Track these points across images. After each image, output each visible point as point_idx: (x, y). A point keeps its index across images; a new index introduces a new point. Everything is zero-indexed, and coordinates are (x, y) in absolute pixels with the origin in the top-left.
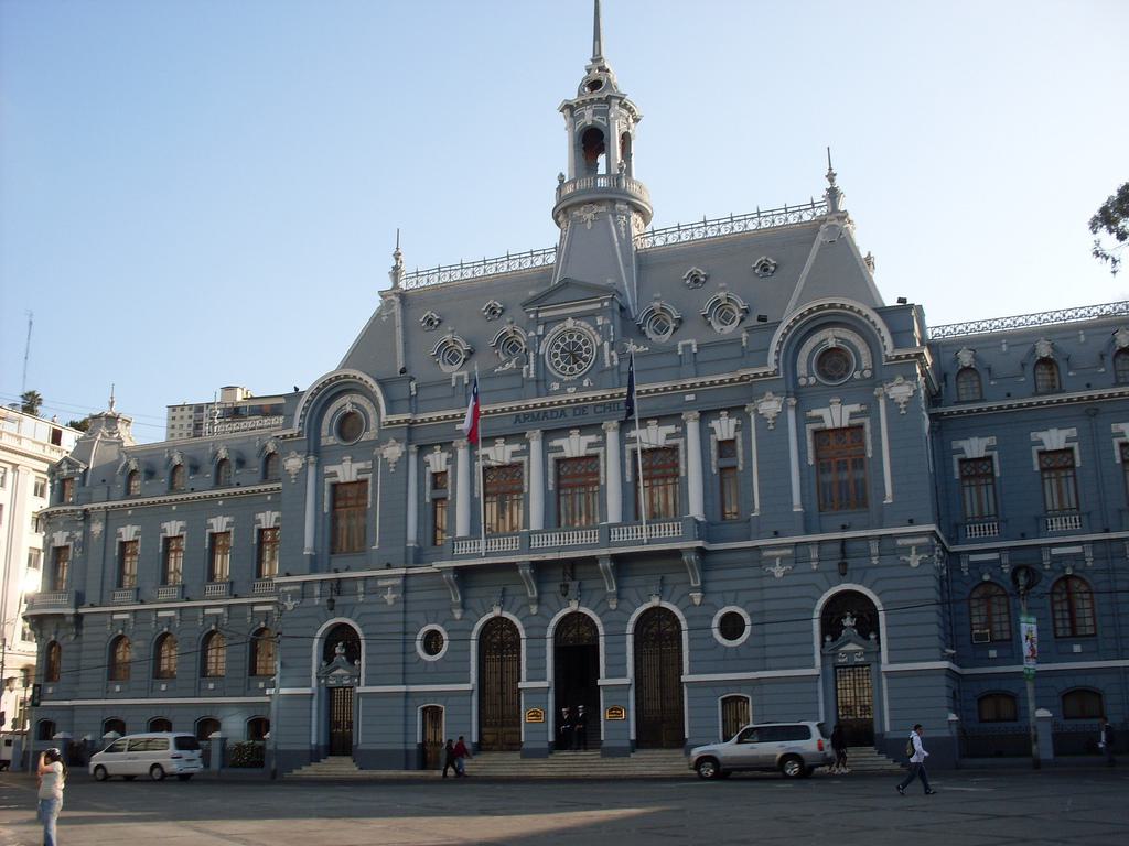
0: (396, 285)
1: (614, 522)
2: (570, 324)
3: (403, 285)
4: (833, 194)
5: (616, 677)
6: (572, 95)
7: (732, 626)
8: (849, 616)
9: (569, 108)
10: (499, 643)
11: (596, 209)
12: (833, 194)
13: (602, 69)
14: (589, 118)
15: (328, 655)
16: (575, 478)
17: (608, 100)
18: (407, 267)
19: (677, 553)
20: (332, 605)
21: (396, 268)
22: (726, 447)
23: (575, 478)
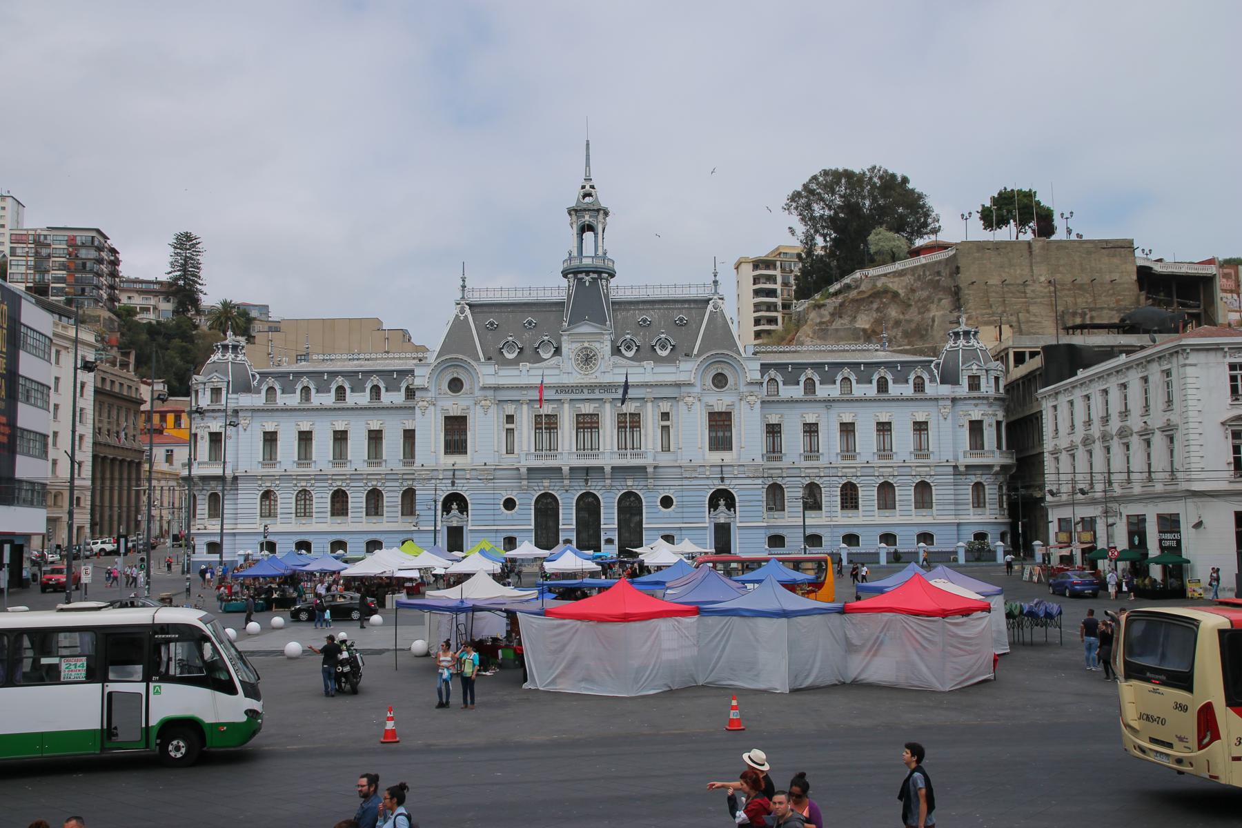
0: (463, 298)
1: (608, 451)
2: (586, 345)
3: (468, 294)
4: (715, 282)
5: (609, 521)
6: (573, 204)
7: (667, 502)
8: (721, 498)
9: (575, 211)
10: (546, 509)
11: (592, 275)
12: (715, 282)
13: (592, 187)
14: (587, 218)
15: (447, 508)
16: (587, 424)
17: (598, 210)
18: (468, 284)
19: (645, 468)
20: (453, 484)
21: (463, 287)
22: (665, 416)
23: (587, 424)
